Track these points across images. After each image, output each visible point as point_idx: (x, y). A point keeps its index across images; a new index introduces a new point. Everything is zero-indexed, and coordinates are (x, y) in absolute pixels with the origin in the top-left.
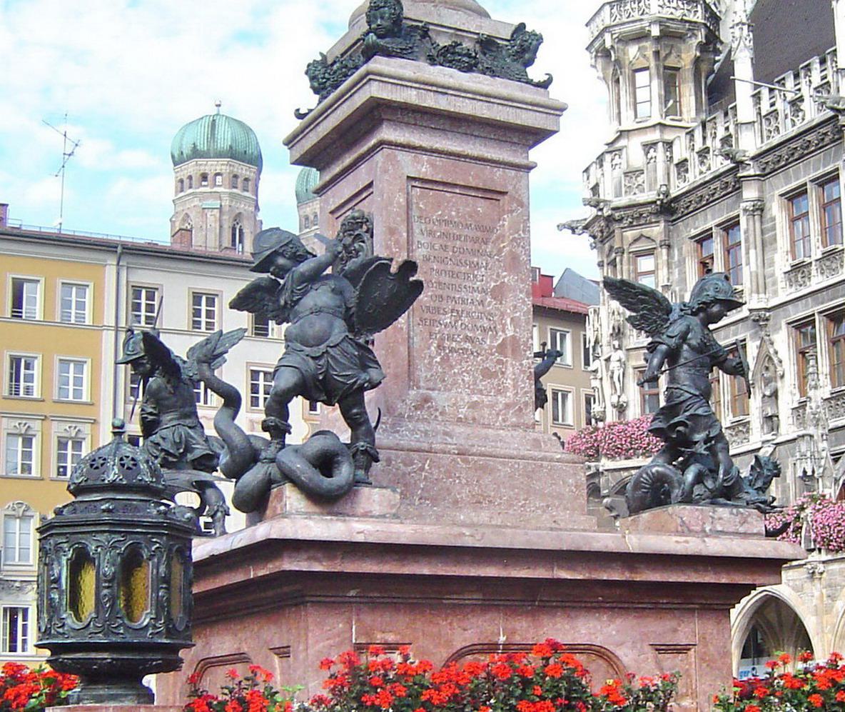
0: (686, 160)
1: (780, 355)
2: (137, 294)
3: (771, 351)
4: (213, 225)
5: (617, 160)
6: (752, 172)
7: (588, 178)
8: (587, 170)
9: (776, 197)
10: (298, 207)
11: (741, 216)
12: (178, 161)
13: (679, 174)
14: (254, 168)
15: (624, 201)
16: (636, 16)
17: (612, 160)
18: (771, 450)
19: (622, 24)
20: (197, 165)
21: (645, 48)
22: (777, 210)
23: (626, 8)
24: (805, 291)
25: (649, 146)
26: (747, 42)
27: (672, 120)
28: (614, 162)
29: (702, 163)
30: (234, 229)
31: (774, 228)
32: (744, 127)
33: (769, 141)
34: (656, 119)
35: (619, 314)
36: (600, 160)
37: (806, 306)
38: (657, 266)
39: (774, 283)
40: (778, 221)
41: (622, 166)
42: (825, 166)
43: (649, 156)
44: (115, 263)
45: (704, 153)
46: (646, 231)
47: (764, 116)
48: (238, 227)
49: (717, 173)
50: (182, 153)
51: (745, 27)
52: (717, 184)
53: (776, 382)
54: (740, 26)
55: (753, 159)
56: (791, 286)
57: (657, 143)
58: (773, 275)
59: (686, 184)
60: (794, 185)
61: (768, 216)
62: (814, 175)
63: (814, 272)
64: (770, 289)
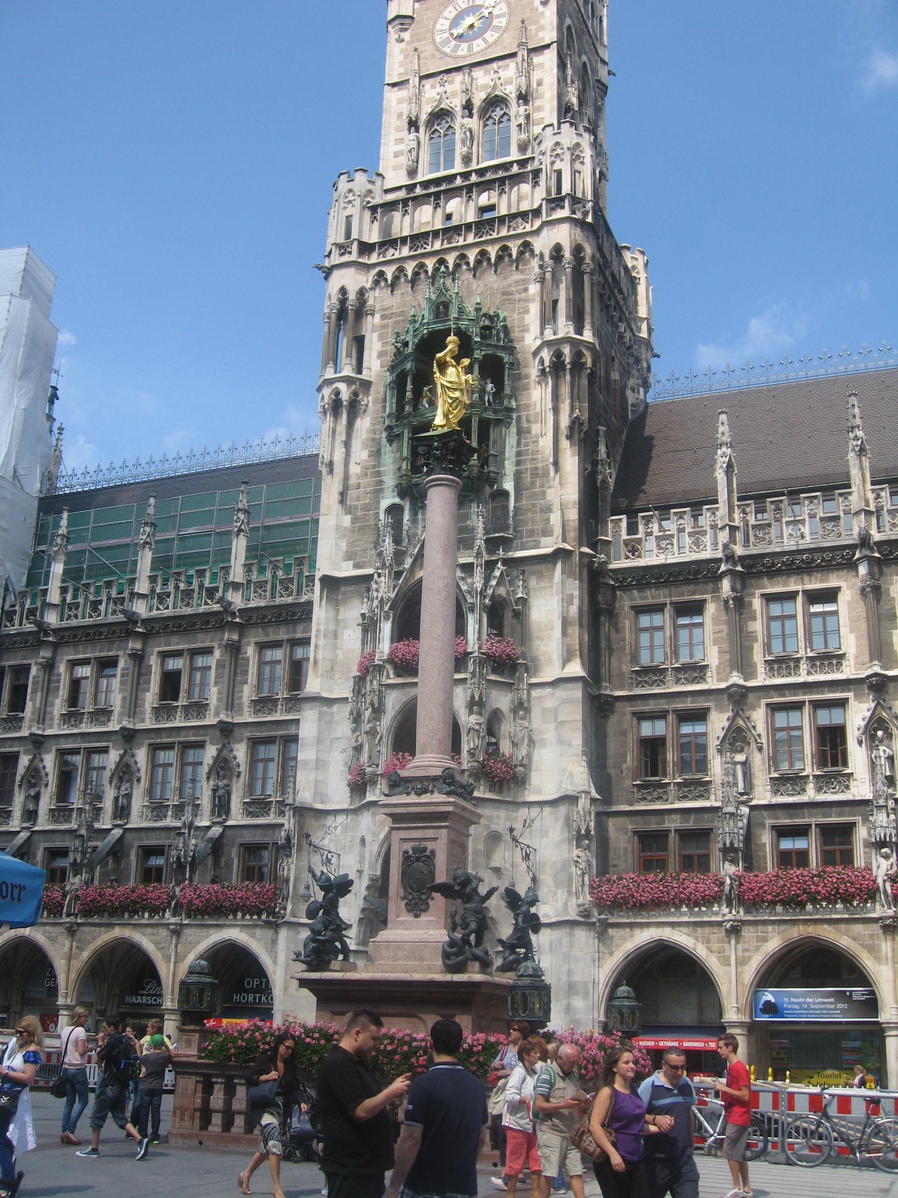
1: (47, 770)
3: (41, 766)
6: (51, 639)
9: (65, 662)
18: (28, 834)
31: (59, 681)
37: (75, 742)
39: (52, 719)
40: (63, 675)
42: (108, 651)
49: (20, 631)
52: (19, 639)
53: (40, 788)
55: (53, 630)
58: (52, 713)
60: (81, 656)
61: (56, 671)
62: (98, 654)
63: (85, 720)
64: (47, 722)
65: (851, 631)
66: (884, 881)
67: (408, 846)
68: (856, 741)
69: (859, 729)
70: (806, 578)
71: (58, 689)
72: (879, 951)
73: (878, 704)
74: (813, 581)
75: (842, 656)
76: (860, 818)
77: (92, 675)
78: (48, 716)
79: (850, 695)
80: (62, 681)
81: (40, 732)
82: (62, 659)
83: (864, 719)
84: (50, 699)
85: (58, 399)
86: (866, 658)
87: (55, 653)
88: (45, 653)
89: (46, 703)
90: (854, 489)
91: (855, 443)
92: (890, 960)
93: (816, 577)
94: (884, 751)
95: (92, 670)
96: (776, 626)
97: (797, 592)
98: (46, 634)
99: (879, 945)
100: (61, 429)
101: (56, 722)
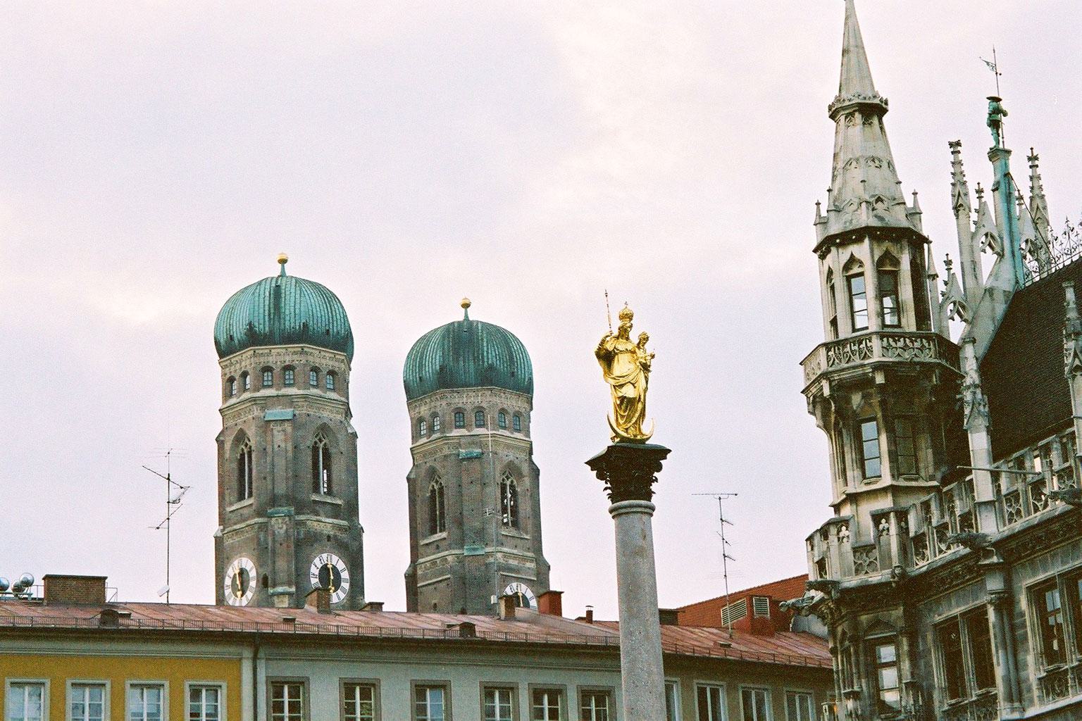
0: (923, 534)
2: (279, 694)
4: (283, 445)
5: (844, 532)
6: (995, 559)
7: (812, 549)
8: (810, 539)
9: (1024, 591)
10: (409, 405)
11: (989, 606)
12: (225, 349)
13: (916, 549)
14: (341, 356)
15: (852, 582)
16: (858, 361)
17: (838, 534)
19: (843, 370)
20: (255, 354)
21: (871, 395)
22: (1023, 603)
23: (845, 350)
24: (1062, 703)
25: (877, 518)
26: (981, 408)
27: (906, 479)
28: (841, 535)
29: (941, 540)
30: (315, 449)
31: (1024, 625)
32: (983, 508)
33: (1012, 525)
34: (887, 480)
35: (857, 715)
36: (824, 532)
38: (898, 655)
39: (1029, 690)
40: (1027, 617)
41: (850, 541)
43: (881, 527)
44: (251, 655)
45: (942, 529)
46: (882, 615)
47: (1005, 496)
48: (321, 445)
50: (232, 338)
51: (979, 391)
54: (972, 389)
56: (1048, 694)
57: (889, 513)
59: (925, 563)
60: (1041, 577)
61: (1017, 610)
64: (1026, 695)
71: (1026, 639)
77: (1063, 604)
78: (1024, 686)
80: (1028, 623)
81: (1016, 716)
82: (1021, 587)
84: (1021, 657)
85: (1005, 115)
87: (1008, 582)
88: (994, 584)
89: (1017, 665)
95: (1062, 596)
98: (988, 554)
100: (1033, 158)
101: (1036, 693)
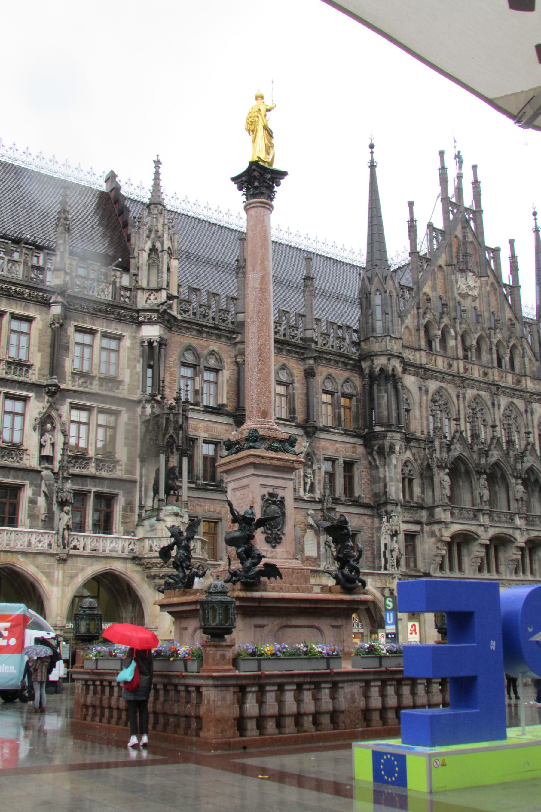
65: (39, 351)
66: (64, 529)
67: (265, 491)
68: (32, 428)
69: (35, 420)
70: (14, 306)
72: (53, 576)
73: (51, 405)
74: (18, 308)
75: (29, 367)
76: (28, 482)
79: (32, 395)
83: (40, 414)
86: (46, 371)
90: (58, 253)
91: (65, 222)
92: (60, 583)
93: (21, 305)
94: (51, 439)
96: (14, 337)
97: (6, 312)
99: (54, 573)
